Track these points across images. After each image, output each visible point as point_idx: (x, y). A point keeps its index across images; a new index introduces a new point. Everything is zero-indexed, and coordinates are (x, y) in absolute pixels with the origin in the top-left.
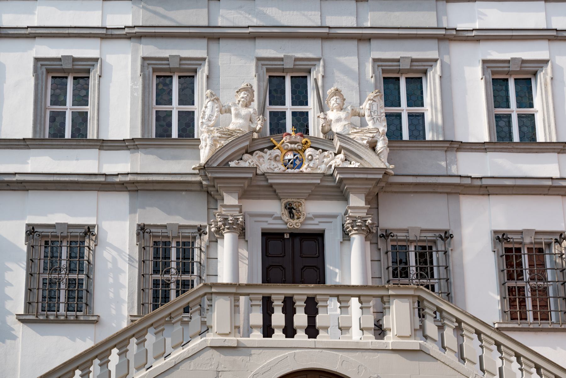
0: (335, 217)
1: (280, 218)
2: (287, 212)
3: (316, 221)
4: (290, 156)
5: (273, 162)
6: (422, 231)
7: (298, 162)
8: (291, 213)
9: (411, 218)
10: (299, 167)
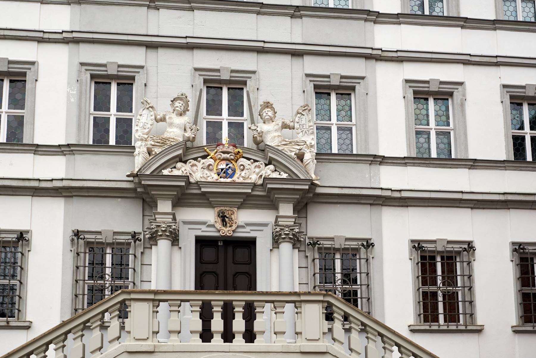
0: (266, 225)
1: (213, 226)
2: (219, 220)
3: (248, 229)
4: (223, 166)
5: (206, 171)
6: (347, 239)
7: (230, 171)
8: (223, 221)
9: (332, 225)
10: (231, 176)
